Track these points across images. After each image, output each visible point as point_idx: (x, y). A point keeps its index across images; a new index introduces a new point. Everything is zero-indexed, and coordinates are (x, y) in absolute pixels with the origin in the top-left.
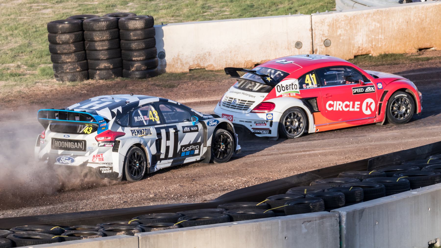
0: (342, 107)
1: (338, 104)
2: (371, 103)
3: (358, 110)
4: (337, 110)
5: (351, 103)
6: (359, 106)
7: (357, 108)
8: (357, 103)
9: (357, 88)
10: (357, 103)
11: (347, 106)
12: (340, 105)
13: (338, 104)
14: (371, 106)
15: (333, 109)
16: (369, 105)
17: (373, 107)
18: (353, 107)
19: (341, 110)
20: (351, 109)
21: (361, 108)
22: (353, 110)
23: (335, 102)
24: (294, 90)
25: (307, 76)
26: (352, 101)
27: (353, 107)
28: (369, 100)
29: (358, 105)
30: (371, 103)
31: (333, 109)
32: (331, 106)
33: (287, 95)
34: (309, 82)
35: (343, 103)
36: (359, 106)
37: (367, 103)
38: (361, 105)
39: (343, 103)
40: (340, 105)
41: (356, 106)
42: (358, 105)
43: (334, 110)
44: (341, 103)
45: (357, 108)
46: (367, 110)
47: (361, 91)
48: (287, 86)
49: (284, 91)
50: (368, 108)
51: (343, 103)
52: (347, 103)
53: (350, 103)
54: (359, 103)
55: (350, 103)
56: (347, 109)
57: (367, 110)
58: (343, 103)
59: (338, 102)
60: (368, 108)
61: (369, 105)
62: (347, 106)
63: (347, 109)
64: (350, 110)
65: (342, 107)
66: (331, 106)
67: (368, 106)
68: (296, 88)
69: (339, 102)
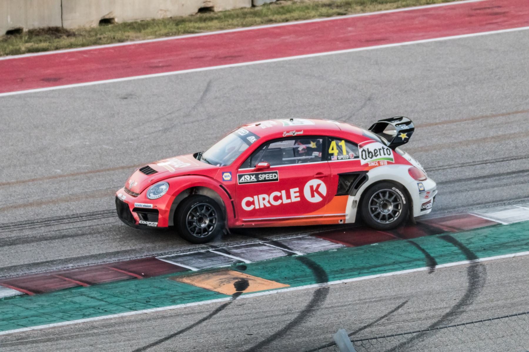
0: (269, 202)
1: (261, 199)
2: (318, 186)
3: (298, 199)
4: (262, 206)
5: (284, 192)
6: (298, 194)
7: (296, 197)
8: (292, 191)
9: (265, 173)
10: (292, 191)
11: (276, 198)
12: (264, 199)
13: (261, 199)
14: (320, 190)
15: (255, 208)
16: (314, 189)
17: (323, 189)
18: (288, 197)
19: (268, 205)
20: (285, 201)
21: (302, 195)
22: (289, 201)
23: (256, 197)
24: (387, 156)
25: (333, 144)
26: (283, 190)
27: (288, 197)
28: (314, 182)
29: (295, 192)
30: (318, 186)
31: (255, 208)
32: (248, 204)
33: (376, 164)
34: (336, 152)
35: (269, 196)
37: (312, 187)
38: (301, 192)
39: (269, 196)
40: (264, 199)
42: (295, 192)
43: (257, 207)
44: (265, 196)
45: (296, 197)
46: (313, 196)
47: (269, 177)
48: (376, 151)
49: (371, 158)
50: (315, 194)
51: (269, 196)
52: (278, 194)
53: (281, 192)
54: (297, 189)
55: (281, 192)
57: (313, 196)
58: (269, 196)
59: (259, 196)
60: (315, 194)
61: (314, 189)
62: (276, 198)
63: (279, 202)
64: (284, 202)
65: (269, 202)
66: (248, 204)
67: (314, 191)
68: (389, 153)
69: (261, 196)
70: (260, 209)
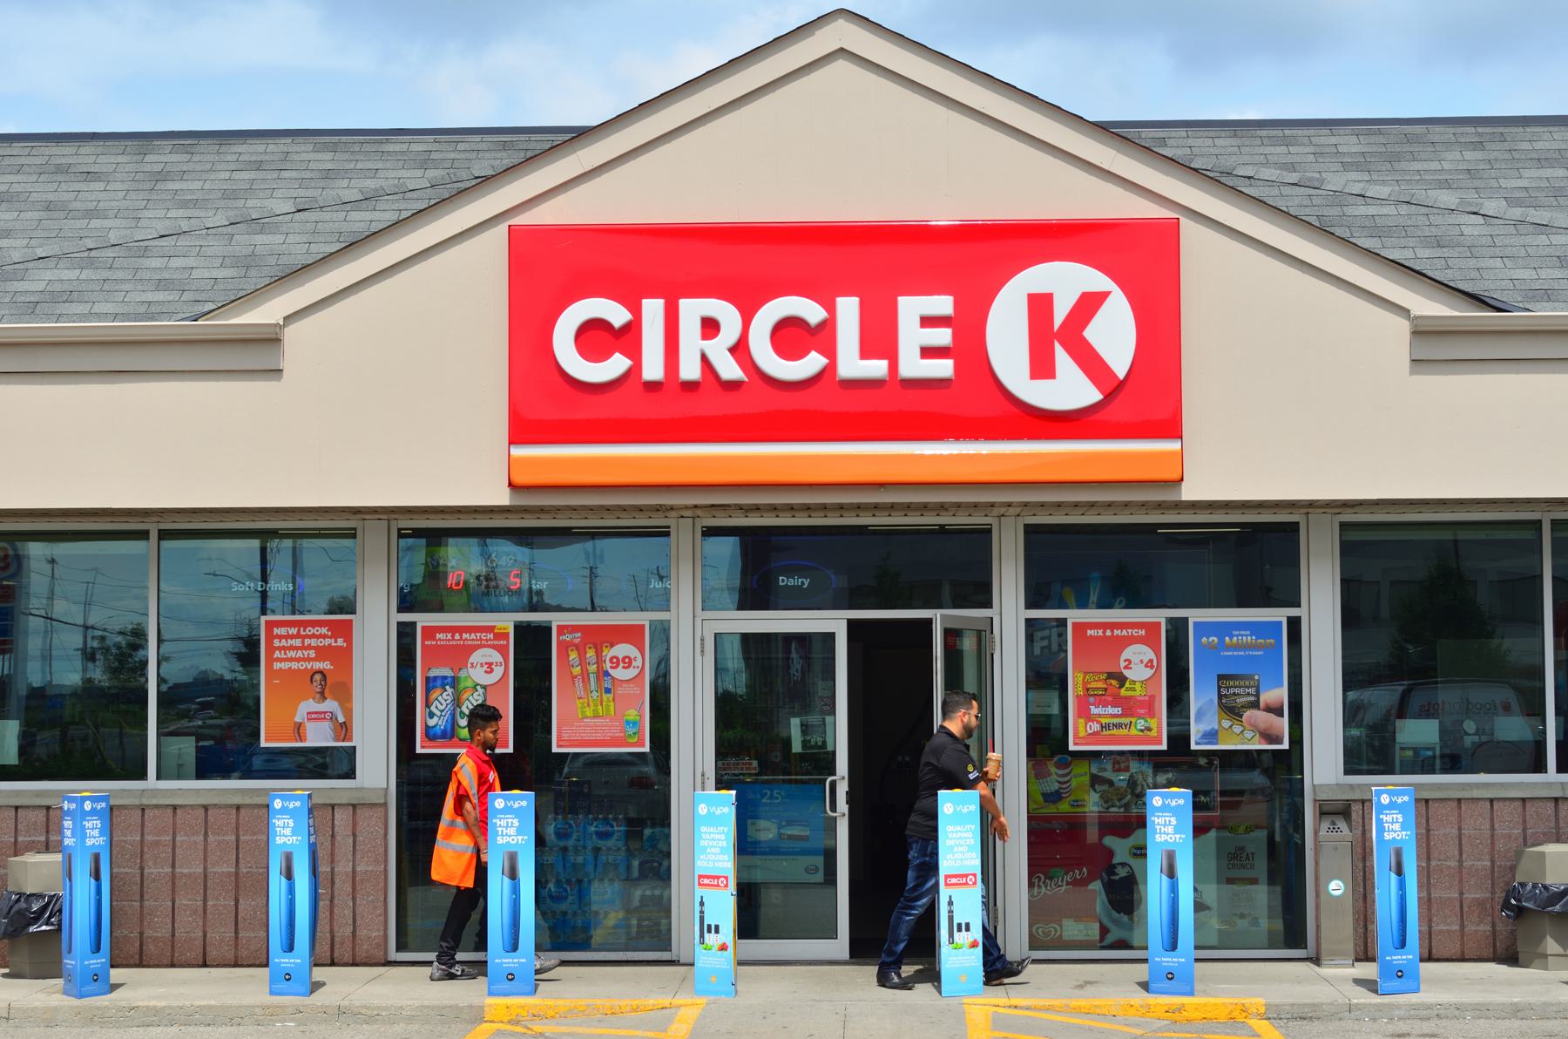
0: (740, 349)
2: (1089, 304)
3: (943, 368)
4: (690, 370)
5: (848, 309)
6: (943, 336)
7: (928, 352)
8: (911, 308)
10: (911, 308)
11: (790, 337)
12: (710, 327)
14: (1094, 333)
15: (636, 368)
16: (1060, 314)
18: (879, 340)
19: (730, 369)
20: (853, 365)
27: (879, 340)
29: (928, 322)
30: (1089, 304)
32: (595, 337)
36: (943, 336)
37: (1040, 305)
40: (710, 327)
41: (911, 337)
42: (928, 322)
43: (653, 369)
44: (726, 312)
45: (928, 352)
50: (1062, 358)
54: (943, 305)
56: (812, 363)
57: (1042, 367)
60: (1062, 357)
61: (1060, 314)
62: (790, 337)
63: (812, 363)
65: (740, 349)
66: (595, 337)
69: (692, 310)
70: (672, 384)
